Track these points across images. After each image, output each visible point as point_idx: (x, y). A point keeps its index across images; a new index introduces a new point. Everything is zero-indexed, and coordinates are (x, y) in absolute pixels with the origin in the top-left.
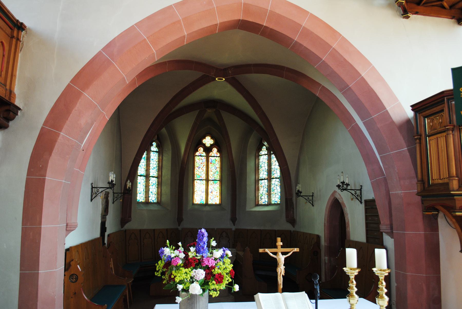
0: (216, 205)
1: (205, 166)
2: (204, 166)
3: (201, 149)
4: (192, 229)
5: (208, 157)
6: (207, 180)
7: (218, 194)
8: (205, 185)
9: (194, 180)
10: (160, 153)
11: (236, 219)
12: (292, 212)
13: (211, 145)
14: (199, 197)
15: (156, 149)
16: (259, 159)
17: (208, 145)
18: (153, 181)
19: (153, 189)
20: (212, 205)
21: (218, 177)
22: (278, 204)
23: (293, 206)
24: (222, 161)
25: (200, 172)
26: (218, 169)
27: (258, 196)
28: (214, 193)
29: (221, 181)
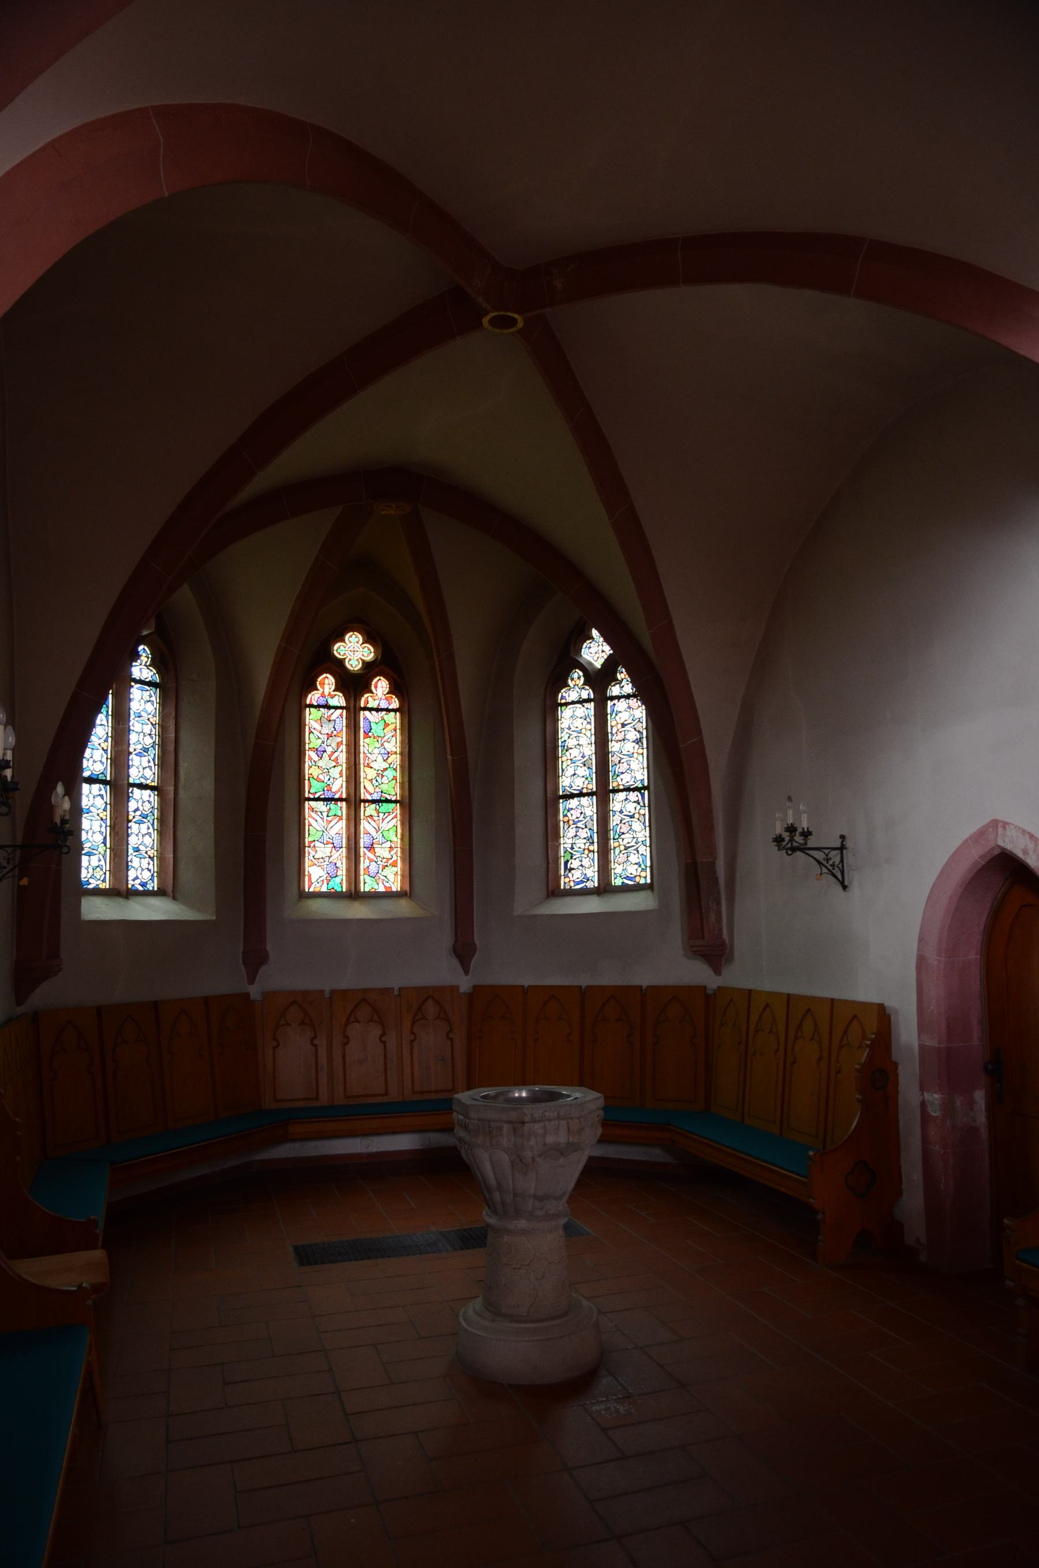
0: (388, 895)
1: (343, 747)
2: (339, 744)
3: (327, 683)
4: (305, 993)
5: (353, 711)
6: (354, 801)
8: (343, 823)
9: (301, 800)
10: (168, 688)
11: (473, 949)
12: (713, 917)
13: (366, 665)
14: (322, 869)
16: (556, 720)
17: (354, 664)
18: (142, 802)
19: (143, 837)
21: (392, 789)
22: (638, 888)
23: (719, 893)
24: (409, 731)
25: (323, 770)
26: (396, 759)
27: (557, 859)
28: (382, 851)
29: (408, 804)
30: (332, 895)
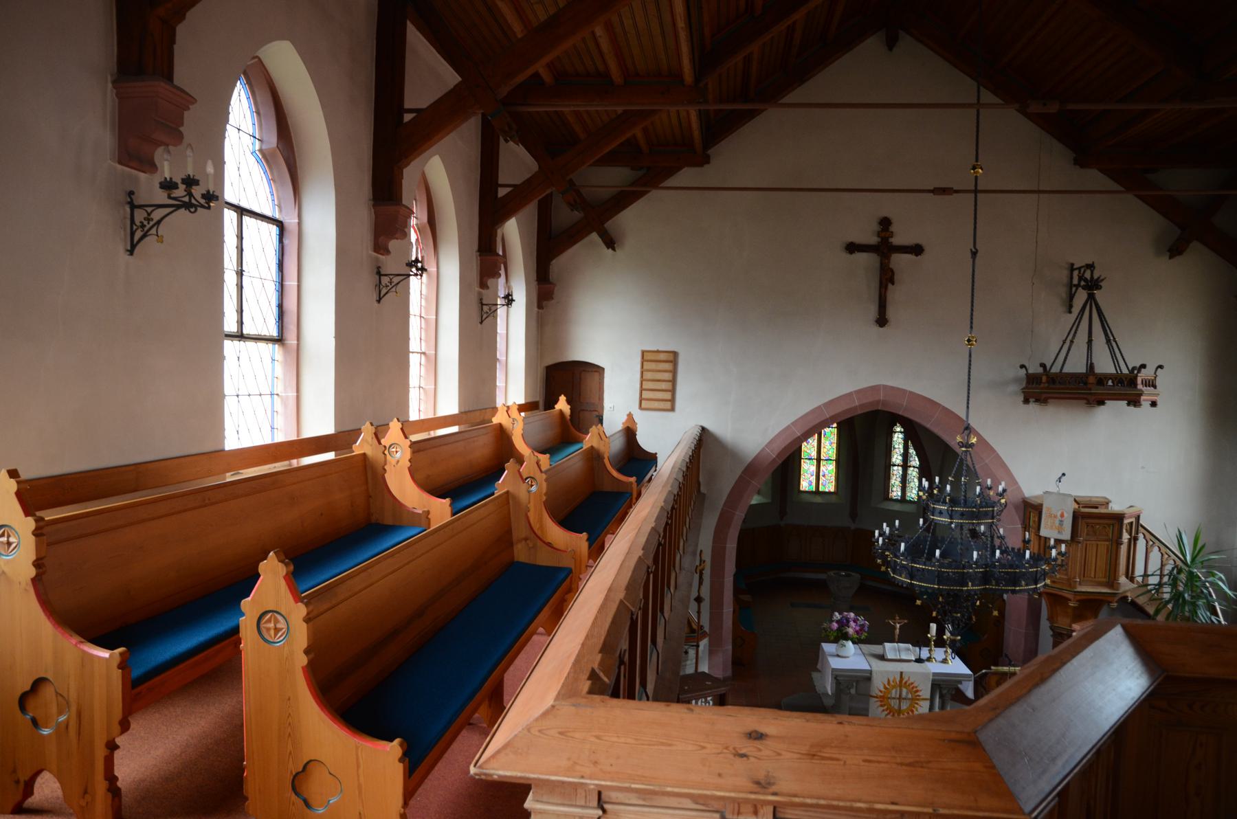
0: (830, 493)
7: (833, 479)
9: (800, 458)
14: (806, 484)
16: (892, 438)
20: (824, 493)
29: (838, 461)
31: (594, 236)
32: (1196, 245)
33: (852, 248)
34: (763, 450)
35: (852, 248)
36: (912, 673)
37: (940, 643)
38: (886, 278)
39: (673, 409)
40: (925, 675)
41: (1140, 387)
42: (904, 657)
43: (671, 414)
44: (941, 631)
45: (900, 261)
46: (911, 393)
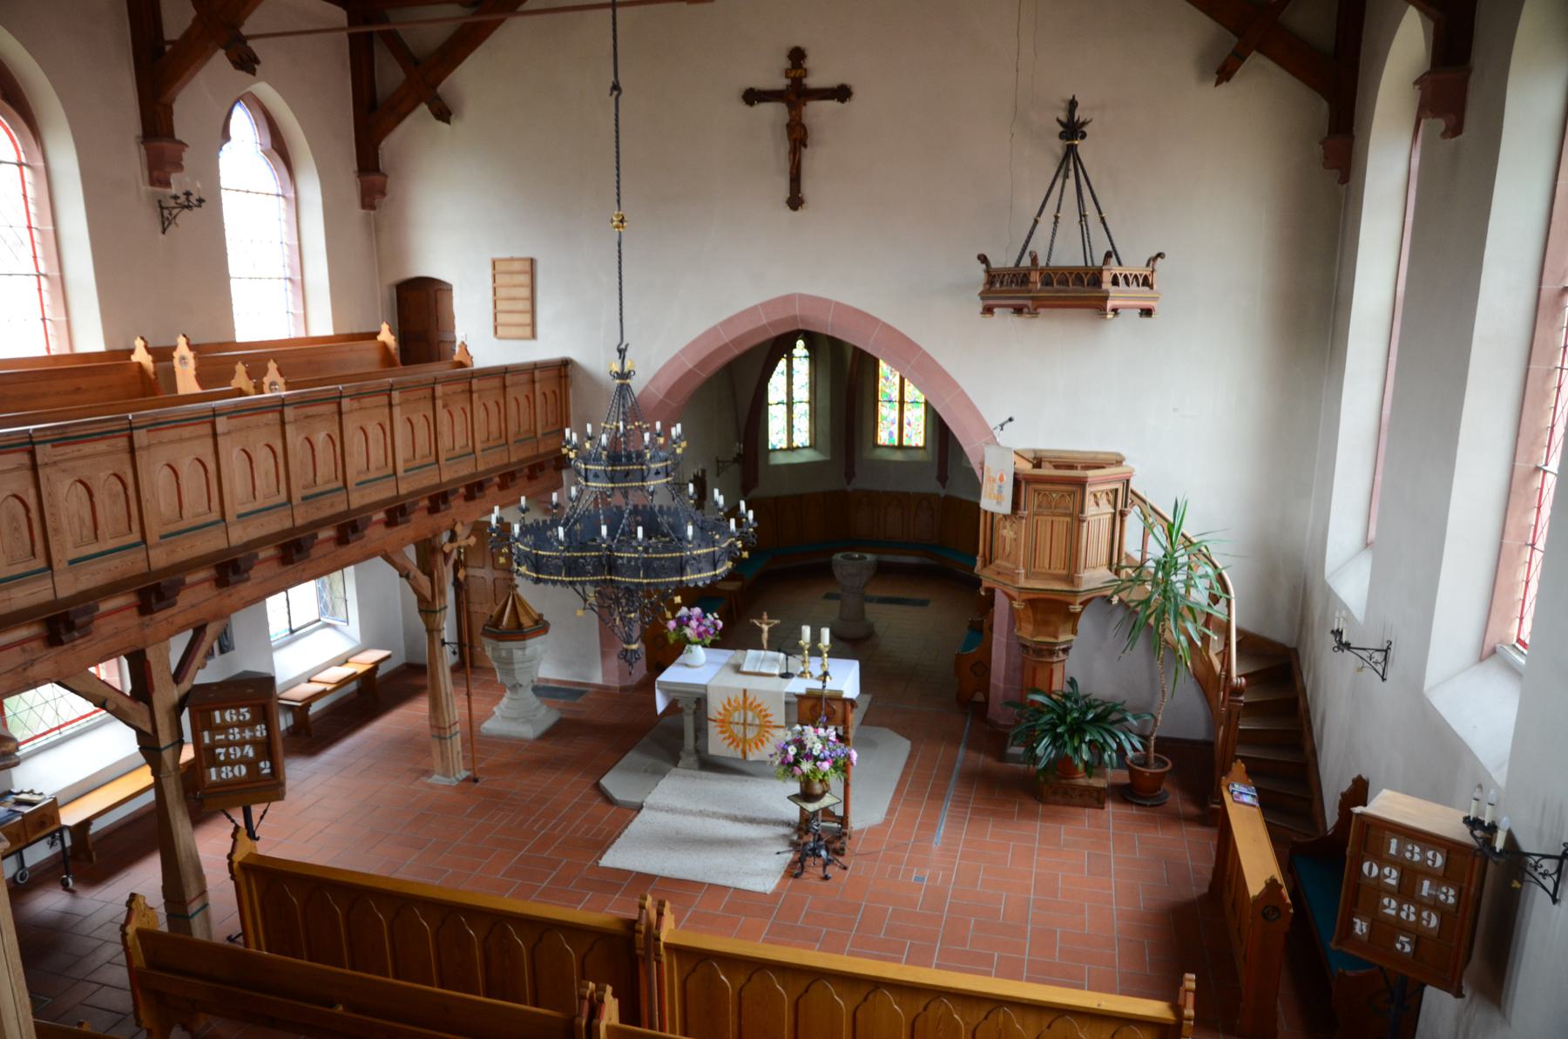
0: (917, 448)
9: (876, 401)
15: (805, 352)
20: (910, 448)
30: (892, 447)
31: (423, 108)
32: (1256, 60)
33: (752, 97)
34: (646, 387)
35: (752, 97)
36: (761, 692)
37: (815, 651)
38: (798, 137)
39: (534, 336)
40: (778, 694)
41: (1107, 285)
42: (764, 670)
43: (532, 343)
44: (816, 637)
45: (818, 113)
46: (838, 305)
